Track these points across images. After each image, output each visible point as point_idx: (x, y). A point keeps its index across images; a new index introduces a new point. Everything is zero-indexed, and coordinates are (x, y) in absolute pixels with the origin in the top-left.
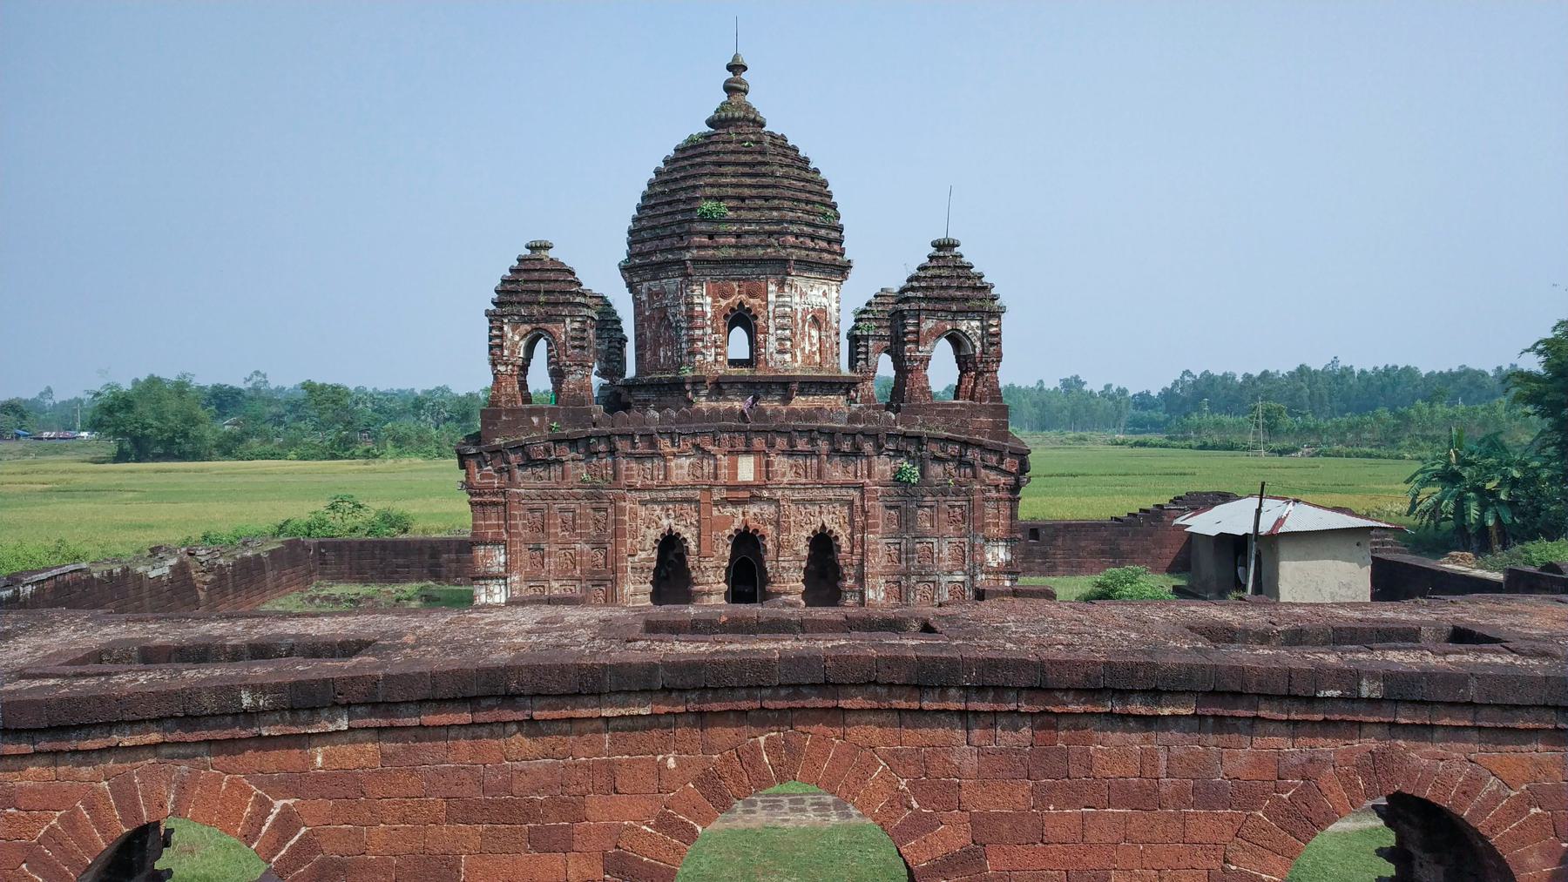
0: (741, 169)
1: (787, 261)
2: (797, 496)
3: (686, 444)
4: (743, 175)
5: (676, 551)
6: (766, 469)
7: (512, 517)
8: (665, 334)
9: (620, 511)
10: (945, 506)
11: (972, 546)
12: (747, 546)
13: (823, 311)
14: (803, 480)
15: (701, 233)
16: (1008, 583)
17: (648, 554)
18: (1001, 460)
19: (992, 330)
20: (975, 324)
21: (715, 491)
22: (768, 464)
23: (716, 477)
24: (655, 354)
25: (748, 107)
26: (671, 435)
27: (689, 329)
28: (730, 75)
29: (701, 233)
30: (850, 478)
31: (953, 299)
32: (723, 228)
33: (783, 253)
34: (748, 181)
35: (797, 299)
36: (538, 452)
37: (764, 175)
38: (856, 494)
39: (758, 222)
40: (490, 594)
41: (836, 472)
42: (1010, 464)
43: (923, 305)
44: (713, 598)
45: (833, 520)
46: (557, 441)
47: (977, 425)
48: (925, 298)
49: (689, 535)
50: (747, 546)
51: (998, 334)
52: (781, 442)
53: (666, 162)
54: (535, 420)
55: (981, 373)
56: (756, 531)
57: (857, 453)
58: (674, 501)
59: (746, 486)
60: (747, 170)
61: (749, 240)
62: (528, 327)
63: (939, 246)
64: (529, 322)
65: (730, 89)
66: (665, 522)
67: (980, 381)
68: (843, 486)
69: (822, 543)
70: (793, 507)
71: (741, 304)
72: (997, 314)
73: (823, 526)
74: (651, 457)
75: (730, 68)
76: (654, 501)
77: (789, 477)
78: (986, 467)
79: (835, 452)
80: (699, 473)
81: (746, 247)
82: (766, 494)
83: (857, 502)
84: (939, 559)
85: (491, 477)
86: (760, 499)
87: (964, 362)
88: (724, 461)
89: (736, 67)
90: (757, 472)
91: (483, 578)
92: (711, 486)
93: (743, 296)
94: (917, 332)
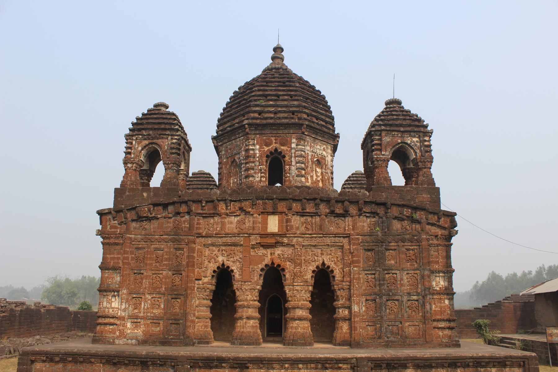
0: (277, 84)
1: (302, 125)
3: (234, 207)
4: (279, 86)
6: (285, 225)
7: (126, 252)
8: (233, 170)
9: (193, 250)
10: (404, 249)
11: (423, 277)
13: (324, 158)
14: (309, 232)
15: (255, 112)
16: (447, 302)
17: (208, 281)
18: (439, 219)
19: (426, 143)
20: (415, 139)
21: (253, 237)
22: (288, 221)
24: (228, 182)
26: (225, 200)
27: (246, 163)
29: (255, 112)
30: (341, 231)
31: (401, 125)
32: (266, 109)
33: (301, 122)
34: (281, 88)
35: (308, 148)
36: (145, 210)
37: (290, 86)
38: (346, 241)
39: (286, 106)
40: (110, 302)
41: (333, 226)
42: (443, 221)
43: (383, 127)
44: (250, 310)
45: (329, 259)
46: (155, 205)
47: (421, 199)
48: (383, 125)
49: (234, 268)
51: (430, 146)
52: (296, 206)
53: (239, 89)
54: (145, 194)
55: (421, 169)
56: (279, 266)
57: (345, 214)
58: (226, 245)
59: (273, 235)
60: (282, 84)
61: (282, 115)
62: (146, 142)
63: (388, 103)
64: (149, 139)
65: (273, 58)
66: (220, 259)
67: (421, 173)
68: (336, 235)
69: (323, 276)
70: (303, 250)
71: (276, 150)
72: (429, 134)
73: (323, 264)
74: (212, 216)
75: (275, 50)
76: (213, 245)
77: (303, 229)
78: (429, 224)
79: (332, 212)
80: (243, 227)
81: (280, 118)
82: (285, 240)
83: (346, 247)
84: (402, 285)
85: (116, 228)
86: (282, 244)
87: (407, 174)
88: (260, 218)
89: (278, 49)
91: (105, 291)
92: (250, 235)
93: (278, 145)
94: (380, 145)
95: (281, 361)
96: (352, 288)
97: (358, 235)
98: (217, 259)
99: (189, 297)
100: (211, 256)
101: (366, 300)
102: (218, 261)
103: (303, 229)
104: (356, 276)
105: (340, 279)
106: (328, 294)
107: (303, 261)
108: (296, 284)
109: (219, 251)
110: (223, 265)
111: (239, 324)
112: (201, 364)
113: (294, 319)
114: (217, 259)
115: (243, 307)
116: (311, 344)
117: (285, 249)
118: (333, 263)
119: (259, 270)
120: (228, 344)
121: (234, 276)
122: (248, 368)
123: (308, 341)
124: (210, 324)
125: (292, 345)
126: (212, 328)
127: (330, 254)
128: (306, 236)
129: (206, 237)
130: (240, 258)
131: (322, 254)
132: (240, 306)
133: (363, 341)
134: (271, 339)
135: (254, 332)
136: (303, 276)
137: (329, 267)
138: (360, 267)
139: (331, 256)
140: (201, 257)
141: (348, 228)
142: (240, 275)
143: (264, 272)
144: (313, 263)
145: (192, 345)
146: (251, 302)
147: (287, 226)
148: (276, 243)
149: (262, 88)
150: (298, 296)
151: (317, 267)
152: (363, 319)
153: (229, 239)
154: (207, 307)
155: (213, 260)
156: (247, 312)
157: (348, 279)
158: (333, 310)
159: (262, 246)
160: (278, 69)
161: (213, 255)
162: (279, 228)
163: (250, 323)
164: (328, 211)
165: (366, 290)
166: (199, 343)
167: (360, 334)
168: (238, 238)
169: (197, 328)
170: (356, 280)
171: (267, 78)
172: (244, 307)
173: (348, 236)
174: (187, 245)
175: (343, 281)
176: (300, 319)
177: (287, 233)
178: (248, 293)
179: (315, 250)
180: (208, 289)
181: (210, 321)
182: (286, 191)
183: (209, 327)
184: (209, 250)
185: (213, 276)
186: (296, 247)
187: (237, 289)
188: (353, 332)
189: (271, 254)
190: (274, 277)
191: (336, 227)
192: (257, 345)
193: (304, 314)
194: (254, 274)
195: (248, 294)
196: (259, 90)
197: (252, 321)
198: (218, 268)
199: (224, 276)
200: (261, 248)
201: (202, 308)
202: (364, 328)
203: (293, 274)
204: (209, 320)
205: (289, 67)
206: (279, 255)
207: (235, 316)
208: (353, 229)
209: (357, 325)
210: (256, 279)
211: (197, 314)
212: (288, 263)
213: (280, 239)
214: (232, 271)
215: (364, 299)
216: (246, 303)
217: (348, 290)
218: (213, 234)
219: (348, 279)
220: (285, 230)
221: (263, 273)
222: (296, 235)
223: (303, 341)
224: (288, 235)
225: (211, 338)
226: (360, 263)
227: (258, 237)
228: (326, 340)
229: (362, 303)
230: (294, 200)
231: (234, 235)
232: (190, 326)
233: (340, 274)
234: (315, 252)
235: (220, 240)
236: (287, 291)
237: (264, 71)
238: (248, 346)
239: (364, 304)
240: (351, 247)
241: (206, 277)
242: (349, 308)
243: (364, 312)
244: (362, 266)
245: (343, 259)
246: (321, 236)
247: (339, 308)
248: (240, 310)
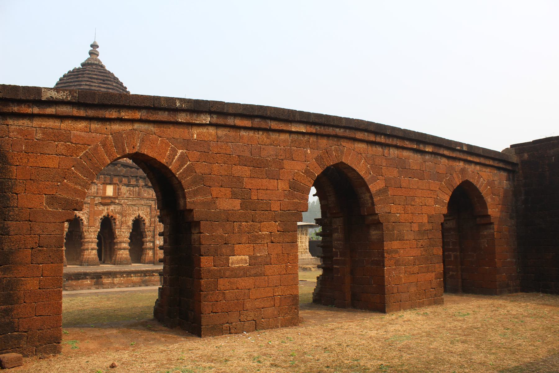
2: (130, 203)
4: (100, 83)
6: (117, 192)
12: (107, 224)
21: (96, 198)
22: (119, 189)
23: (97, 193)
25: (99, 61)
28: (92, 49)
37: (109, 84)
50: (107, 224)
52: (125, 180)
59: (110, 197)
60: (102, 82)
65: (91, 53)
68: (148, 199)
69: (138, 223)
73: (139, 216)
75: (92, 46)
82: (117, 201)
86: (115, 203)
88: (101, 187)
89: (95, 46)
90: (114, 192)
95: (121, 273)
103: (128, 194)
112: (73, 278)
113: (121, 249)
115: (88, 242)
116: (130, 264)
117: (116, 206)
122: (101, 278)
137: (142, 218)
147: (118, 192)
149: (88, 83)
151: (135, 218)
158: (143, 243)
160: (96, 64)
164: (144, 184)
171: (90, 74)
176: (124, 249)
178: (92, 234)
182: (117, 169)
186: (124, 205)
196: (86, 85)
205: (104, 63)
212: (118, 215)
213: (113, 200)
214: (82, 220)
227: (100, 199)
230: (124, 176)
237: (83, 65)
242: (154, 242)
245: (151, 213)
247: (147, 242)
248: (86, 244)
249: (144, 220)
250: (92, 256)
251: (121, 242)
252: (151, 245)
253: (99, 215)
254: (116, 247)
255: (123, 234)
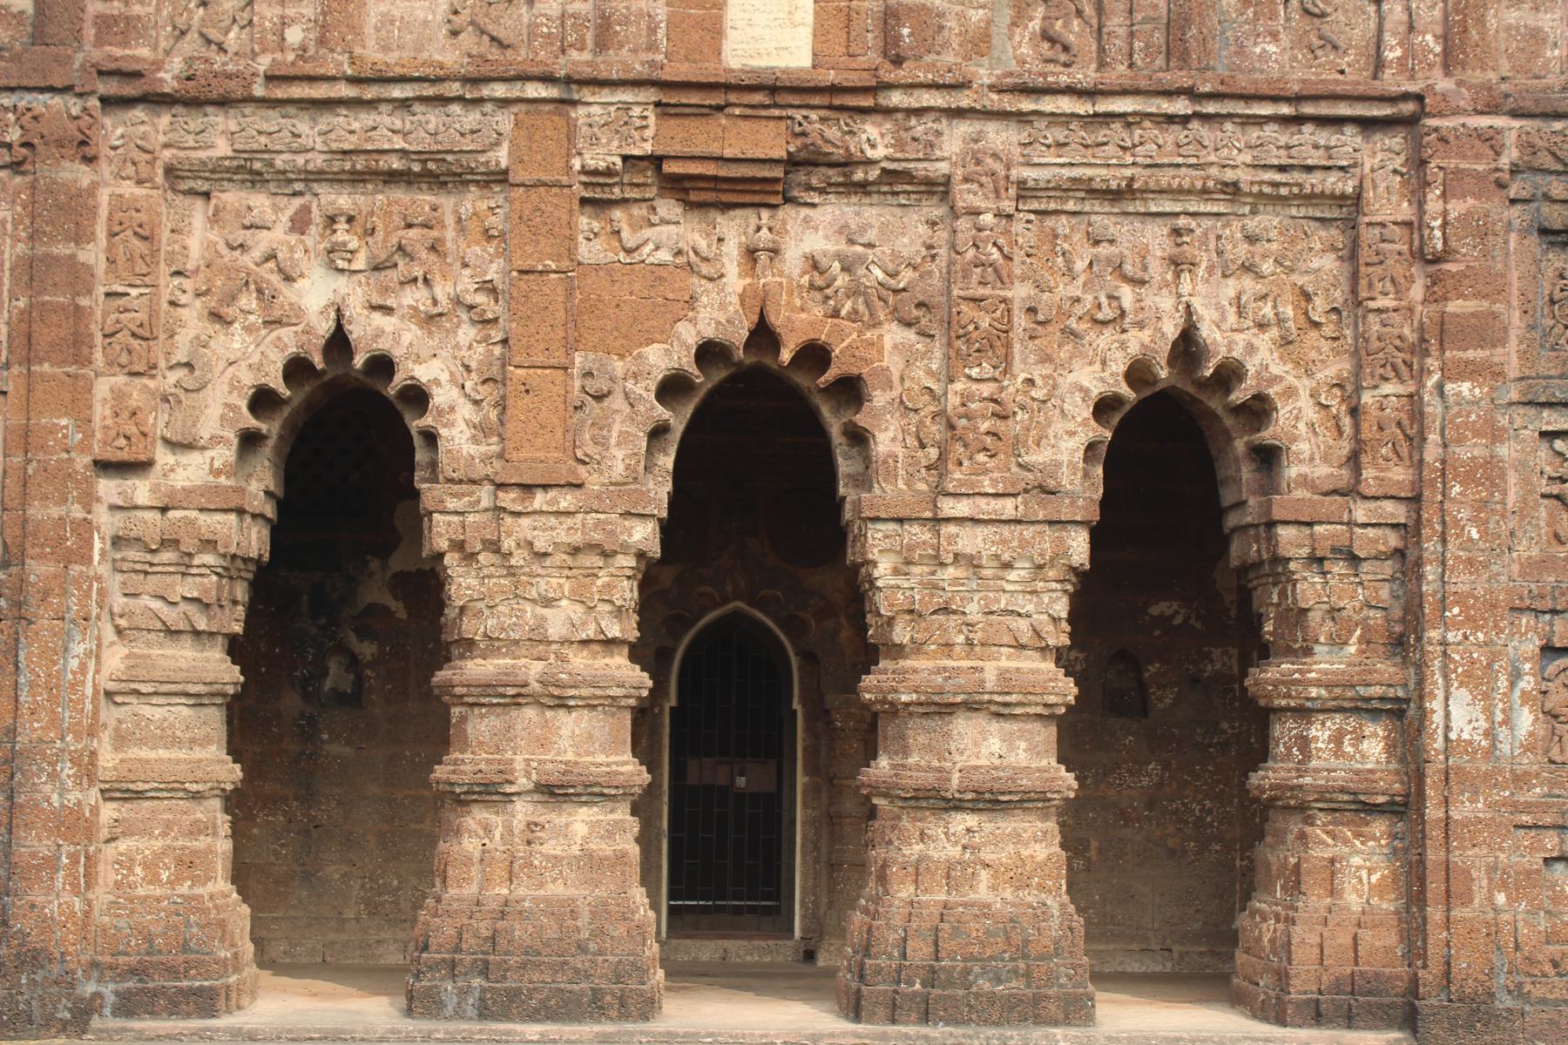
2: (1046, 169)
5: (399, 562)
9: (74, 213)
14: (1085, 75)
17: (208, 484)
21: (595, 108)
38: (1380, 157)
44: (569, 725)
58: (363, 173)
59: (774, 91)
66: (316, 295)
68: (1302, 108)
69: (1174, 458)
70: (1024, 231)
73: (1187, 346)
82: (875, 140)
83: (1388, 205)
86: (848, 177)
96: (1431, 546)
97: (1492, 109)
98: (288, 294)
99: (44, 622)
100: (230, 271)
101: (1550, 650)
102: (299, 312)
104: (1470, 451)
105: (1322, 471)
106: (1159, 608)
107: (1021, 321)
108: (962, 508)
109: (300, 224)
110: (339, 342)
111: (470, 846)
114: (288, 294)
116: (1077, 1011)
117: (870, 215)
118: (1264, 341)
119: (645, 390)
120: (374, 1011)
121: (431, 438)
123: (1052, 978)
124: (224, 846)
125: (925, 1017)
126: (241, 875)
127: (1248, 268)
128: (1048, 105)
129: (190, 100)
130: (489, 288)
131: (1178, 264)
132: (488, 687)
133: (1517, 992)
134: (706, 950)
135: (600, 911)
136: (1017, 444)
137: (1229, 374)
138: (1495, 373)
139: (1248, 282)
140: (145, 278)
141: (1409, 50)
142: (482, 430)
143: (688, 411)
144: (1105, 339)
145: (64, 1027)
146: (580, 661)
148: (793, 163)
150: (973, 609)
151: (1137, 373)
152: (1516, 808)
153: (386, 119)
154: (197, 701)
155: (248, 301)
156: (543, 743)
157: (1399, 474)
158: (1251, 730)
159: (678, 186)
161: (247, 260)
162: (820, 32)
163: (564, 833)
165: (1544, 564)
166: (128, 1006)
167: (1493, 930)
168: (471, 118)
169: (107, 875)
170: (1468, 479)
172: (516, 702)
173: (1405, 117)
174: (16, 166)
175: (1352, 491)
176: (990, 800)
177: (890, 74)
178: (550, 582)
179: (1123, 230)
180: (209, 544)
181: (223, 822)
183: (221, 867)
184: (215, 218)
185: (250, 441)
186: (966, 196)
187: (459, 546)
188: (1435, 913)
189: (751, 253)
190: (761, 461)
191: (1299, 41)
192: (625, 1016)
193: (1021, 756)
194: (601, 425)
195: (549, 597)
197: (584, 812)
198: (297, 369)
199: (344, 449)
200: (668, 208)
201: (153, 712)
202: (1521, 883)
203: (935, 430)
204: (214, 812)
206: (814, 265)
207: (440, 772)
208: (1449, 62)
209: (1472, 858)
210: (619, 469)
211: (108, 759)
212: (893, 335)
213: (829, 133)
214: (418, 397)
215: (1532, 645)
216: (535, 670)
217: (1388, 568)
218: (246, 79)
219: (1399, 474)
220: (873, 57)
221: (678, 420)
222: (964, 100)
223: (1016, 985)
224: (896, 98)
225: (236, 964)
226: (1503, 342)
228: (1134, 966)
229: (1515, 676)
231: (432, 88)
232: (52, 863)
233: (1326, 437)
234: (1123, 248)
235: (307, 129)
236: (883, 570)
238: (551, 1029)
239: (1527, 683)
240: (1433, 204)
241: (188, 446)
242: (1403, 715)
243: (1529, 748)
244: (1513, 368)
246: (1181, 106)
247: (1304, 713)
248: (481, 726)
249: (1258, 410)
250: (556, 889)
251: (941, 709)
252: (1372, 748)
253: (632, 339)
254: (883, 765)
255: (974, 588)
